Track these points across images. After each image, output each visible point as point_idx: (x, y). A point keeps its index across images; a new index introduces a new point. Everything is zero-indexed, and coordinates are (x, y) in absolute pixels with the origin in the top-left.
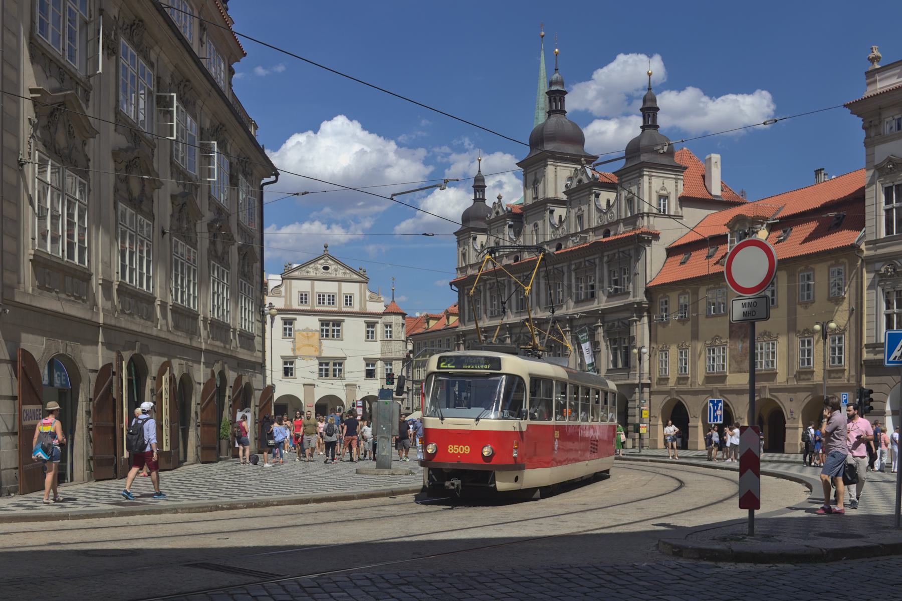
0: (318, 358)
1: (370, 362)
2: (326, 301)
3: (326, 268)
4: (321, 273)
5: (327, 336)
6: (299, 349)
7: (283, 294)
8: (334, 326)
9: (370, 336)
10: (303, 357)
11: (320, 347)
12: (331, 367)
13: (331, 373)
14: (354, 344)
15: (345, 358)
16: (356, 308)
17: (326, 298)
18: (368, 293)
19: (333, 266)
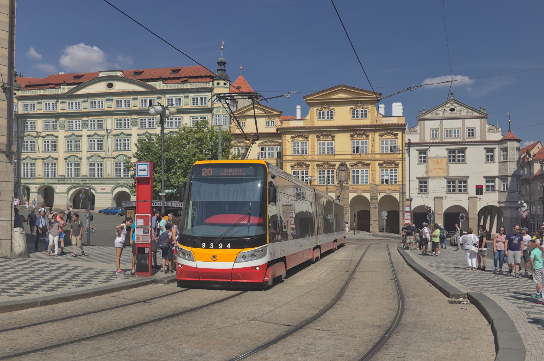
0: (445, 178)
1: (490, 179)
2: (453, 135)
3: (452, 110)
4: (448, 114)
6: (431, 171)
7: (418, 132)
8: (459, 153)
9: (490, 159)
10: (434, 178)
11: (448, 169)
12: (457, 184)
13: (457, 189)
14: (476, 166)
15: (468, 177)
16: (477, 139)
17: (453, 132)
18: (487, 126)
19: (458, 108)
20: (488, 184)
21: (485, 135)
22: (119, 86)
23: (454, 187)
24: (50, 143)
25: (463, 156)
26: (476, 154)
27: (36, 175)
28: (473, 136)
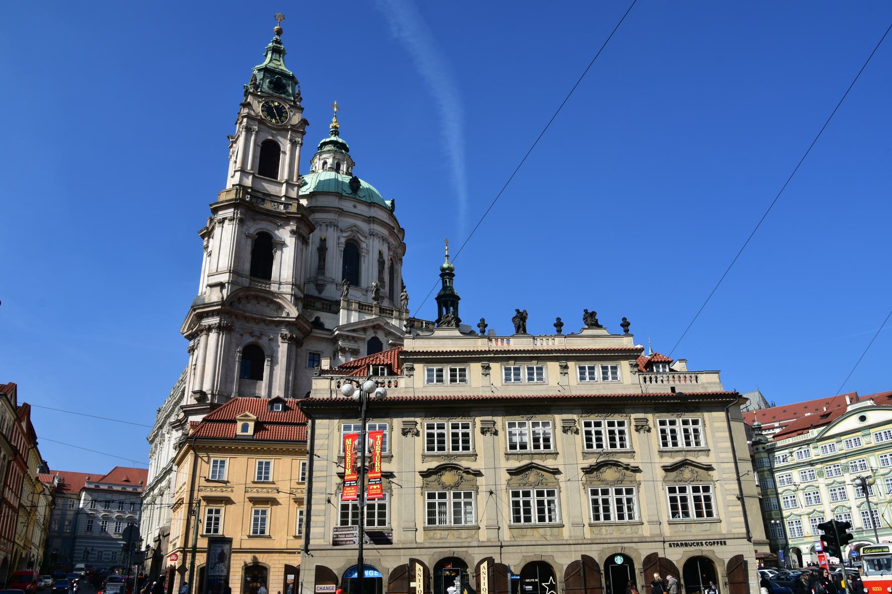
22: (873, 417)
24: (812, 496)
27: (805, 534)
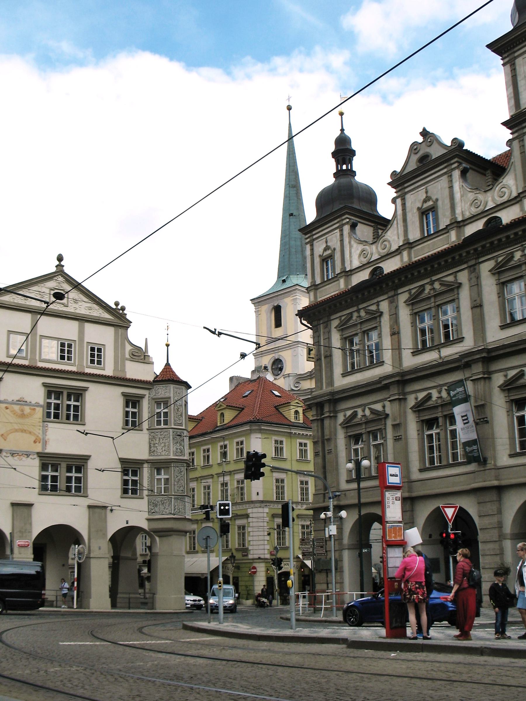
1: (130, 467)
3: (59, 296)
5: (56, 416)
12: (63, 473)
16: (108, 369)
20: (126, 478)
21: (124, 365)
23: (54, 479)
25: (76, 408)
26: (103, 405)
28: (99, 363)
